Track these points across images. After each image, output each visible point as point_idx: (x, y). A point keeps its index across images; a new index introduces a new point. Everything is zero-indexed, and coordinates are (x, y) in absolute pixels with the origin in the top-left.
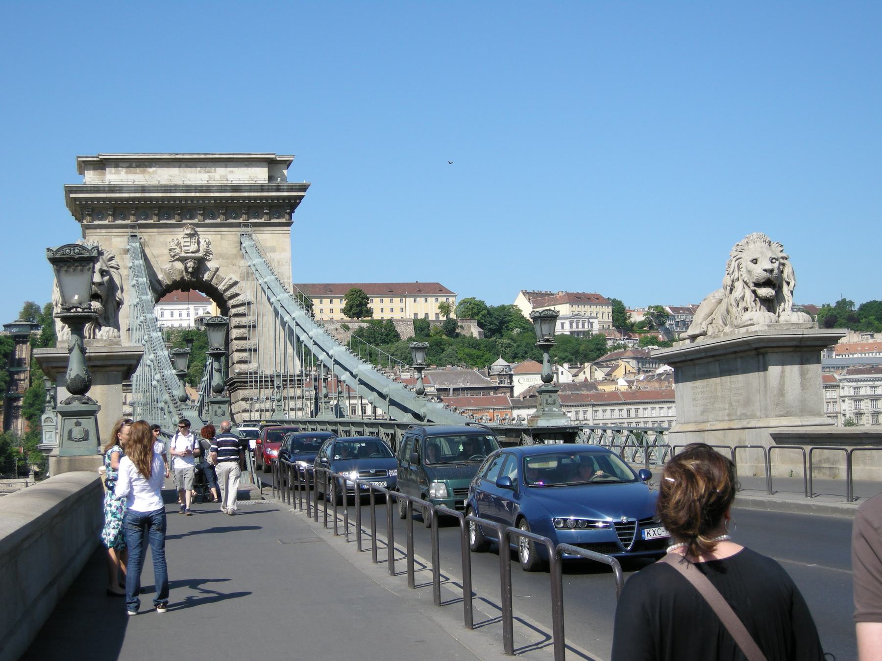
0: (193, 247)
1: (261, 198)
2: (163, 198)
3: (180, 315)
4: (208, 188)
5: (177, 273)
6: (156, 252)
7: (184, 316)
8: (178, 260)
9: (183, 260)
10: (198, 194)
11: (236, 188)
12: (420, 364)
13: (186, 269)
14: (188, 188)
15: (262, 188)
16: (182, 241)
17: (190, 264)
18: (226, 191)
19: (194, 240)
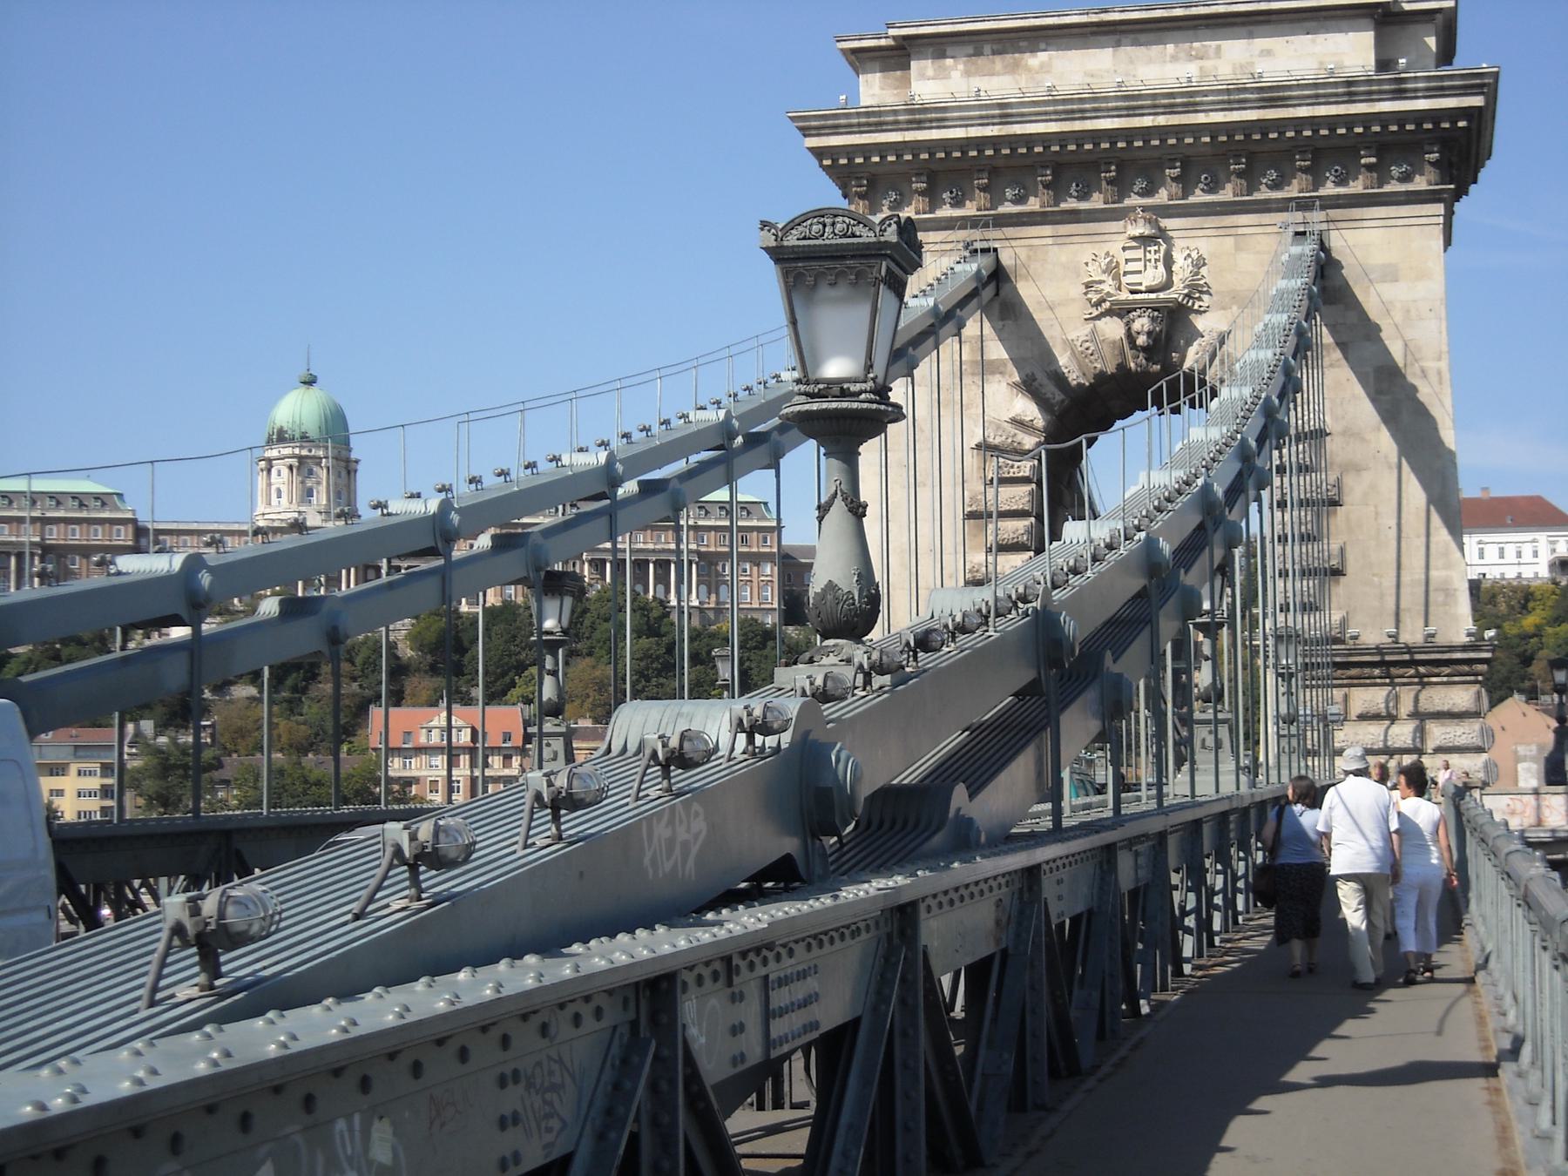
0: (1154, 275)
1: (1349, 120)
2: (1062, 138)
3: (1519, 555)
4: (1189, 100)
5: (1107, 351)
6: (1051, 292)
7: (1527, 556)
8: (1109, 313)
9: (1122, 311)
10: (1162, 120)
11: (1273, 95)
12: (839, 389)
13: (1131, 337)
14: (1132, 103)
15: (1351, 89)
16: (1121, 257)
17: (1142, 323)
18: (1242, 105)
19: (1156, 252)
